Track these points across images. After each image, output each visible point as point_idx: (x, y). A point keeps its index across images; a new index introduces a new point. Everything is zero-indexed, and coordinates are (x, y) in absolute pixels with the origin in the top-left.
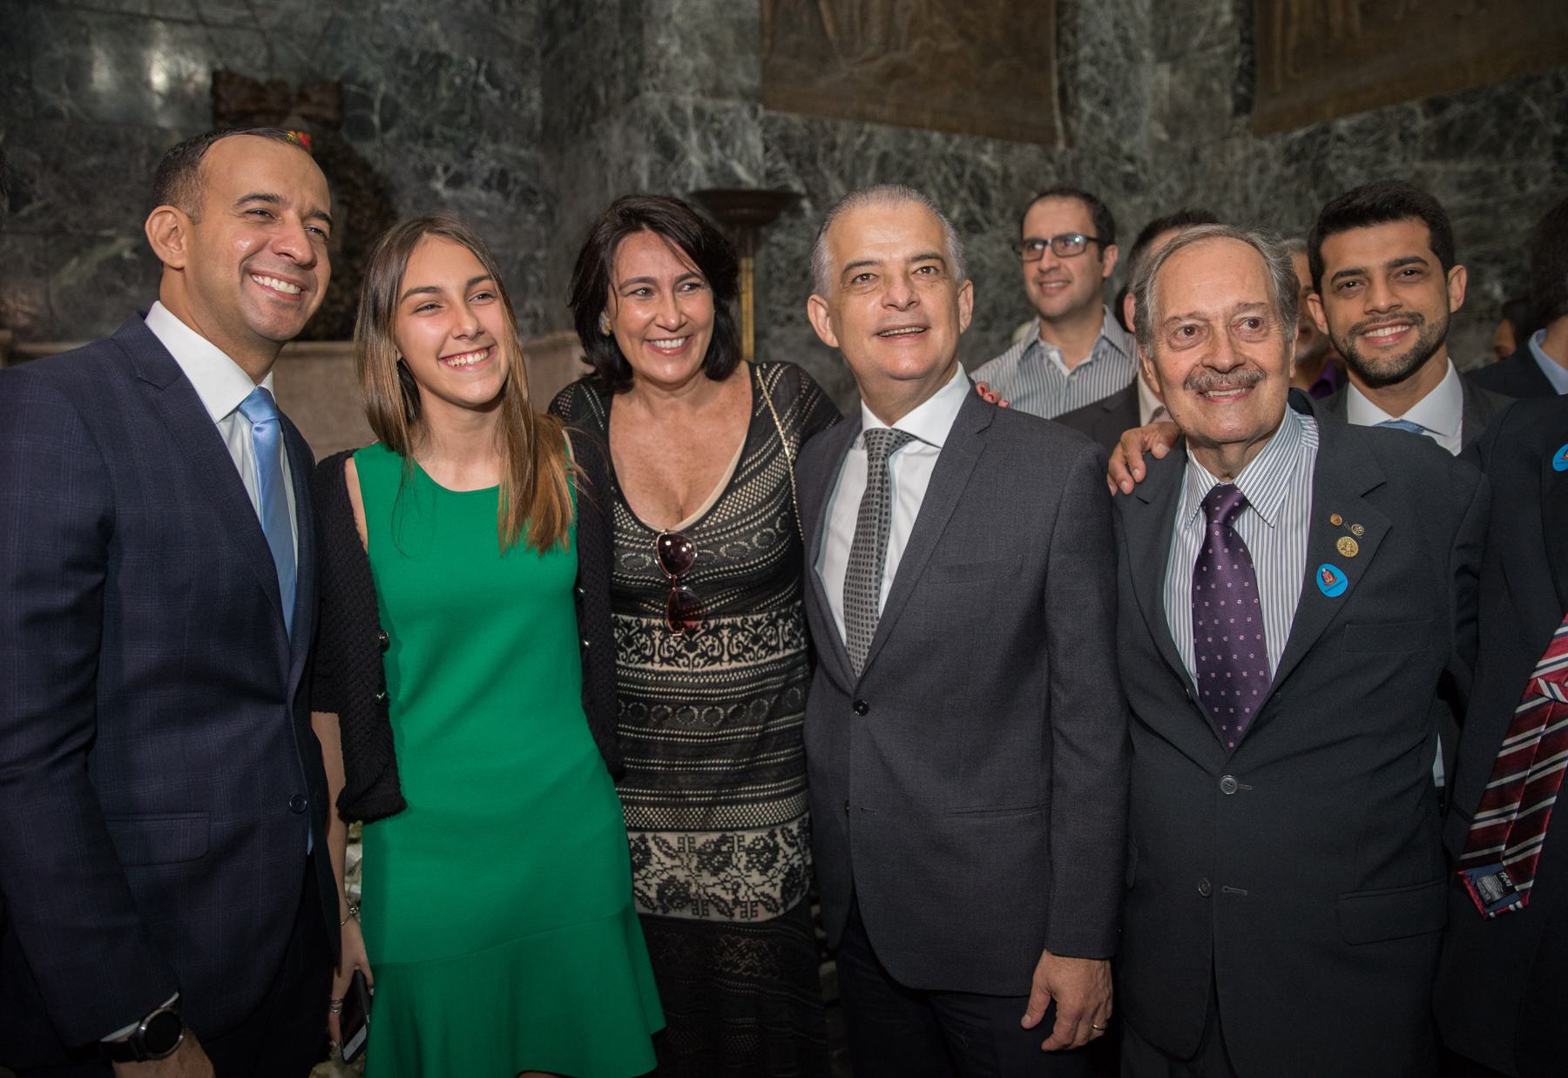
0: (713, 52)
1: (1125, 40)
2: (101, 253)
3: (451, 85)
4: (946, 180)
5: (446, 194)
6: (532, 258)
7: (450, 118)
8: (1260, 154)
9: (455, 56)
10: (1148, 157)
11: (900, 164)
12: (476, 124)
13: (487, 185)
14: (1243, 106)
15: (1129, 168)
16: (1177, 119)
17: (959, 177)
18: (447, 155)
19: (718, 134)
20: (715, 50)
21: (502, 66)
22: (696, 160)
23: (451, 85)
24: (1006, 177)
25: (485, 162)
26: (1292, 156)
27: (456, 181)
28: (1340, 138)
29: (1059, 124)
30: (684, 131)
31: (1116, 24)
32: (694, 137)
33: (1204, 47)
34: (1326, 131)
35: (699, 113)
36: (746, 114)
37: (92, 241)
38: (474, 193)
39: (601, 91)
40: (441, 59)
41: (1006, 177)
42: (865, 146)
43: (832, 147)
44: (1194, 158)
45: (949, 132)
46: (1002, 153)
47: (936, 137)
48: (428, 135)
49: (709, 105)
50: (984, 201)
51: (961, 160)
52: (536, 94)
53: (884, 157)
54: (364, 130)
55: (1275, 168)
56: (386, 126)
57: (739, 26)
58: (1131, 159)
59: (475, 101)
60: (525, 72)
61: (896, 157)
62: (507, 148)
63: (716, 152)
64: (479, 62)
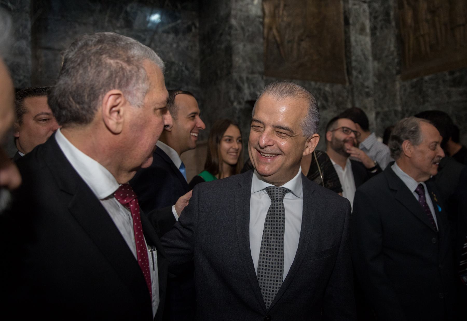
1: (364, 55)
3: (175, 70)
8: (404, 86)
9: (177, 62)
14: (398, 72)
16: (379, 76)
19: (253, 84)
21: (189, 65)
22: (247, 91)
23: (175, 70)
26: (413, 86)
28: (426, 81)
29: (347, 78)
30: (243, 83)
32: (246, 85)
33: (387, 56)
34: (422, 79)
35: (247, 78)
36: (260, 78)
39: (219, 72)
44: (385, 87)
45: (316, 81)
47: (313, 83)
49: (250, 76)
55: (409, 90)
63: (252, 90)
64: (183, 63)
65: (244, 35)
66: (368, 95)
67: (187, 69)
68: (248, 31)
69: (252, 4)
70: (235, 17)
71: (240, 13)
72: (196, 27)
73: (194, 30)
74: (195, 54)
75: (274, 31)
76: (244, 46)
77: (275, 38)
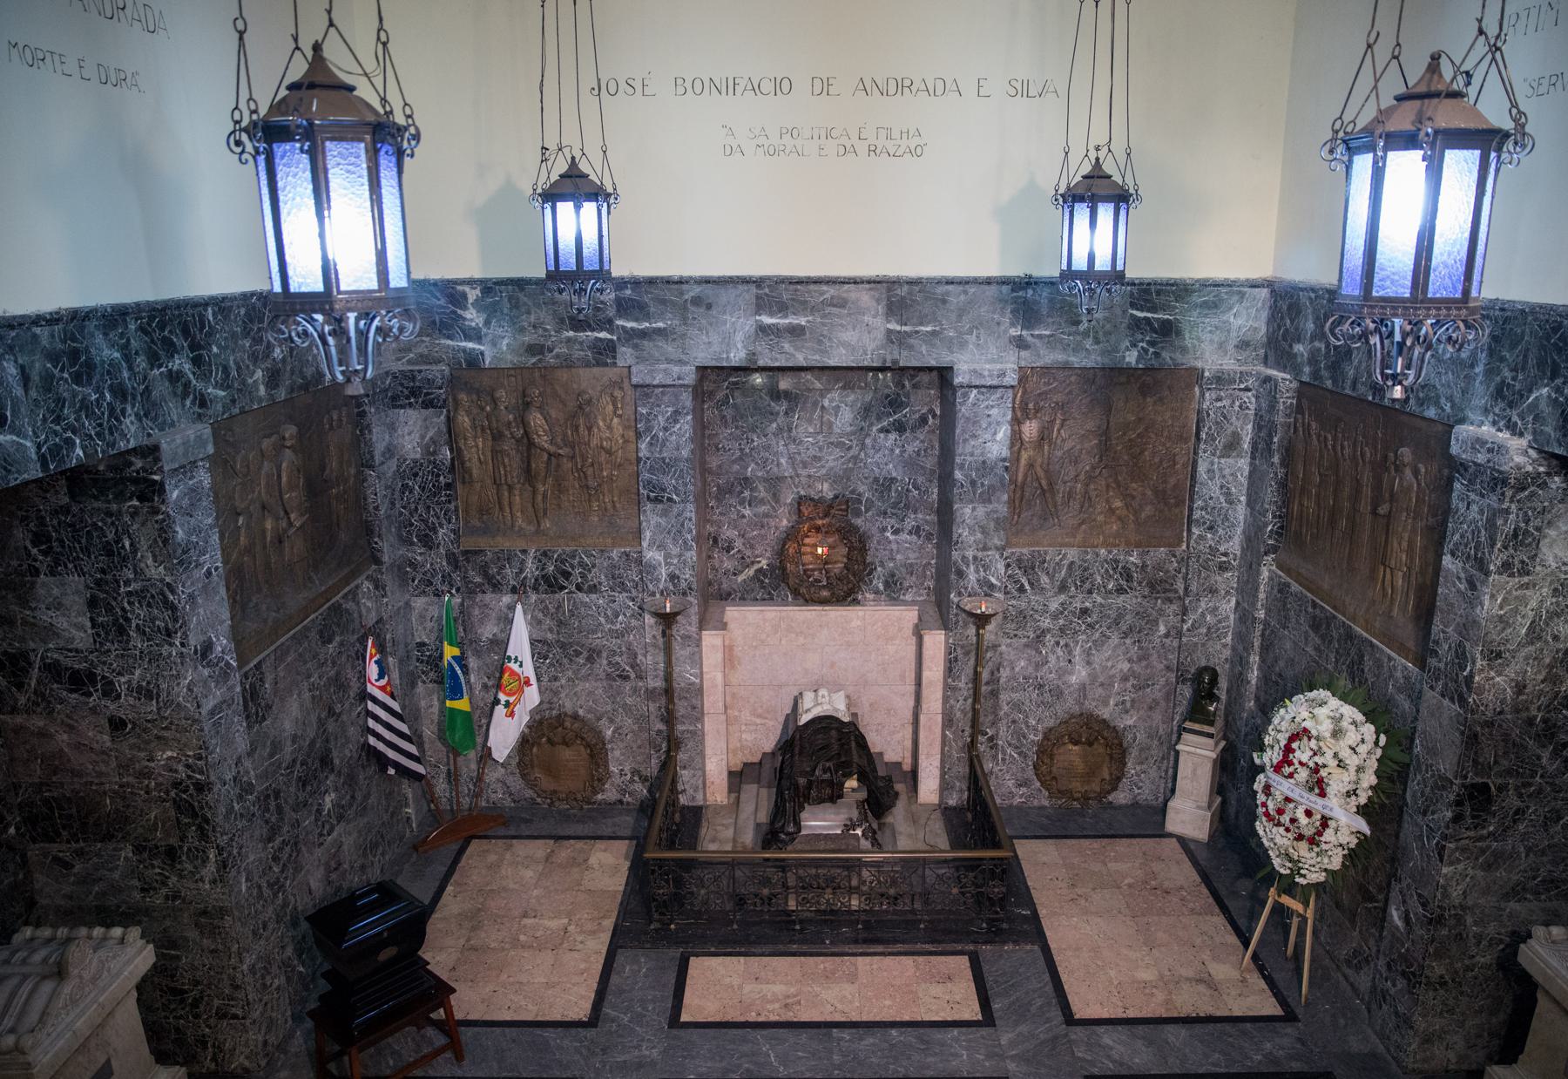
0: (983, 533)
1: (1228, 494)
2: (756, 567)
4: (1107, 570)
5: (892, 538)
6: (929, 564)
7: (895, 505)
10: (1238, 553)
11: (1080, 566)
12: (907, 506)
13: (910, 533)
15: (1224, 559)
17: (1114, 569)
18: (893, 521)
20: (984, 531)
21: (920, 480)
24: (1144, 566)
25: (910, 523)
27: (896, 532)
31: (1222, 487)
32: (972, 567)
35: (975, 558)
36: (997, 557)
37: (753, 563)
38: (904, 536)
40: (893, 480)
41: (1144, 566)
42: (1061, 560)
43: (1045, 561)
46: (1141, 555)
48: (885, 513)
49: (980, 554)
50: (1129, 578)
51: (1117, 561)
52: (936, 490)
53: (1072, 563)
54: (858, 514)
56: (867, 510)
57: (997, 521)
58: (1225, 554)
59: (907, 496)
60: (931, 481)
61: (1078, 563)
62: (920, 516)
63: (982, 573)
65: (974, 494)
66: (1223, 568)
67: (916, 487)
68: (982, 484)
69: (994, 440)
70: (962, 467)
71: (969, 459)
72: (934, 416)
73: (931, 421)
74: (930, 462)
75: (1038, 469)
76: (974, 509)
77: (1038, 479)
